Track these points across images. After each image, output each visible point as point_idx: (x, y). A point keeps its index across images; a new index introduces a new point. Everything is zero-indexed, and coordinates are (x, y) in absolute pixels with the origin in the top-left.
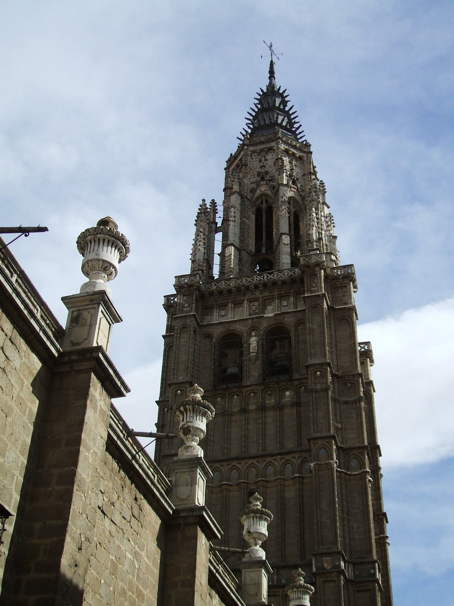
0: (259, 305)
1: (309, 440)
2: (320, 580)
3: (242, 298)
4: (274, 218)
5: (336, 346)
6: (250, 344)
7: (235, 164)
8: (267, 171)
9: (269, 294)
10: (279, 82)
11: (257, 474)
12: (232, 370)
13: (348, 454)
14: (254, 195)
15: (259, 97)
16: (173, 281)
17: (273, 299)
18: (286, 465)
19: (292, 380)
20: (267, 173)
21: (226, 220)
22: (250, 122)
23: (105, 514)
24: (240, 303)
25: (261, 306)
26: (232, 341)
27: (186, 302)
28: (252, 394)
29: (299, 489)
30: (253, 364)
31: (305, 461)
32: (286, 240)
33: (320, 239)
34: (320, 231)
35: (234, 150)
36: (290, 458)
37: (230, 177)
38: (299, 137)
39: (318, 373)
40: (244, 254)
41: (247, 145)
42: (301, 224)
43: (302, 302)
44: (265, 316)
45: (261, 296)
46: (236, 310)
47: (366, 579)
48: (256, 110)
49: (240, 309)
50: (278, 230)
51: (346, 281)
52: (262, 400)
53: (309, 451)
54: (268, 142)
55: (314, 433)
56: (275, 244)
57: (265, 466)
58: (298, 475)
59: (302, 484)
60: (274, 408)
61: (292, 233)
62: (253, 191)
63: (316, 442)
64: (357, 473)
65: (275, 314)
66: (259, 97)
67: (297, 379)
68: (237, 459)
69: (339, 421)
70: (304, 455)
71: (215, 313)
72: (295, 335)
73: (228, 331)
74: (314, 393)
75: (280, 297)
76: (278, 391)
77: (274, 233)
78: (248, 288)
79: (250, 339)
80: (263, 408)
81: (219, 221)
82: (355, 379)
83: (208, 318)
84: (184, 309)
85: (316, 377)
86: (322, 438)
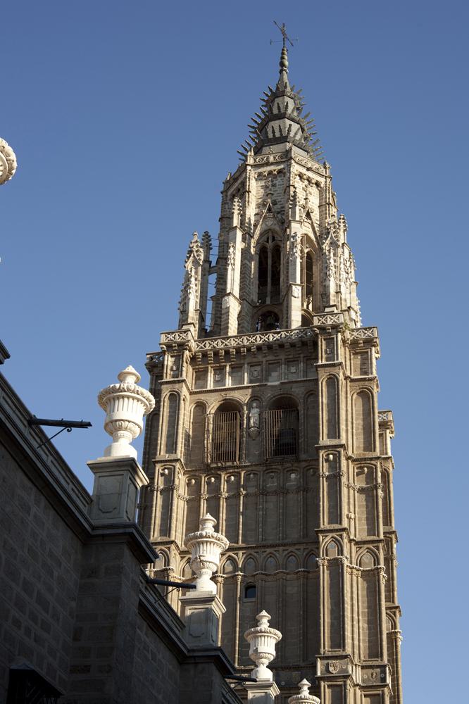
0: (262, 370)
3: (242, 362)
4: (283, 261)
7: (234, 187)
8: (275, 201)
9: (274, 358)
13: (360, 548)
15: (266, 98)
17: (279, 363)
19: (298, 460)
22: (253, 130)
25: (264, 372)
29: (304, 584)
33: (338, 293)
34: (338, 282)
36: (294, 550)
37: (228, 203)
41: (251, 166)
42: (314, 268)
44: (269, 384)
45: (264, 360)
47: (374, 684)
48: (263, 116)
49: (239, 374)
52: (263, 482)
56: (283, 293)
58: (303, 569)
60: (276, 493)
65: (282, 383)
66: (266, 98)
67: (305, 461)
72: (304, 409)
75: (288, 362)
76: (281, 474)
77: (281, 279)
81: (213, 259)
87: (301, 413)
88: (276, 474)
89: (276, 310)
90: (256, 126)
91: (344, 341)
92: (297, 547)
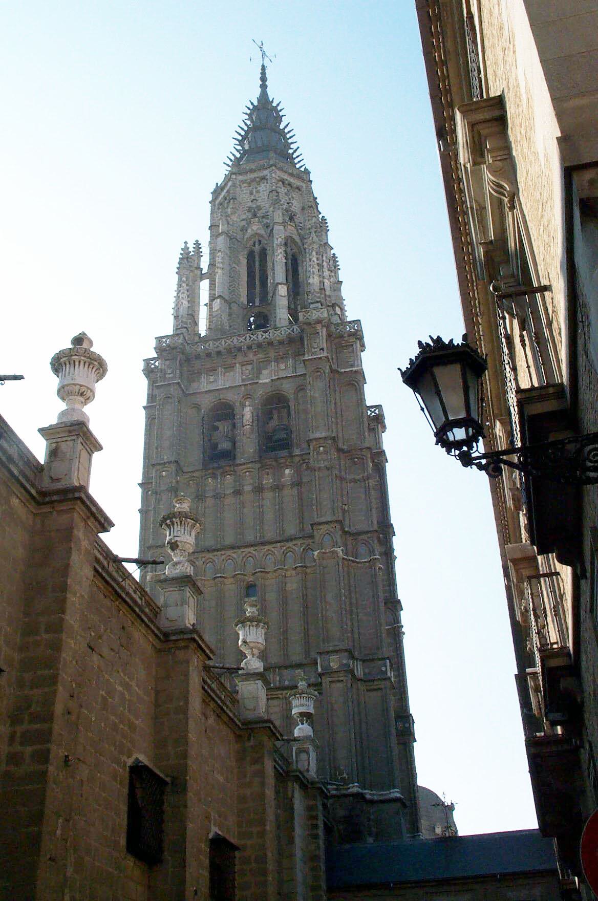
0: (253, 369)
1: (312, 525)
2: (326, 680)
4: (269, 264)
7: (222, 196)
8: (259, 206)
10: (272, 93)
12: (225, 445)
14: (245, 235)
15: (249, 112)
16: (154, 343)
17: (269, 361)
19: (291, 456)
20: (259, 208)
21: (212, 265)
23: (93, 650)
24: (232, 367)
26: (225, 412)
27: (169, 367)
31: (308, 549)
32: (283, 290)
35: (220, 180)
38: (296, 161)
40: (235, 307)
42: (300, 269)
43: (302, 365)
44: (260, 381)
45: (255, 358)
46: (227, 374)
47: (377, 677)
49: (232, 374)
50: (274, 278)
51: (352, 339)
54: (259, 170)
61: (290, 280)
62: (244, 230)
66: (249, 112)
68: (233, 547)
71: (203, 379)
78: (240, 349)
83: (195, 385)
84: (167, 376)
85: (318, 453)
86: (327, 523)
87: (292, 408)
89: (266, 312)
90: (240, 138)
91: (329, 335)
92: (294, 542)
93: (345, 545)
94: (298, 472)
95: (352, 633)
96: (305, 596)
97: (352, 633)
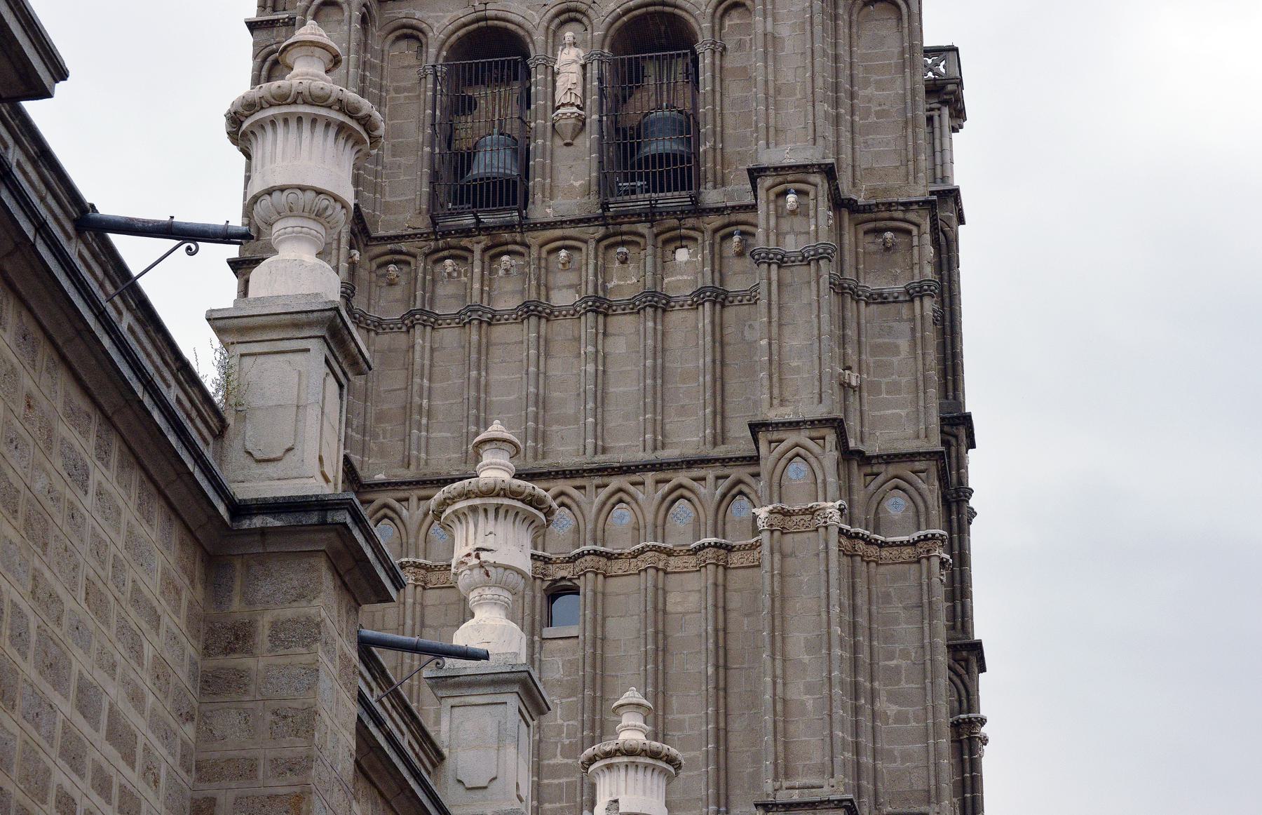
5: (852, 96)
6: (555, 74)
11: (577, 530)
12: (492, 162)
18: (674, 502)
28: (563, 253)
30: (568, 145)
31: (735, 492)
39: (791, 198)
52: (596, 275)
53: (754, 460)
55: (771, 405)
57: (604, 504)
58: (713, 540)
59: (725, 568)
60: (635, 307)
63: (775, 436)
64: (905, 538)
67: (718, 211)
69: (853, 360)
70: (735, 473)
73: (478, 20)
74: (774, 267)
79: (555, 54)
80: (600, 307)
82: (912, 216)
88: (634, 249)
93: (847, 491)
94: (717, 260)
95: (857, 750)
96: (722, 632)
97: (857, 750)
